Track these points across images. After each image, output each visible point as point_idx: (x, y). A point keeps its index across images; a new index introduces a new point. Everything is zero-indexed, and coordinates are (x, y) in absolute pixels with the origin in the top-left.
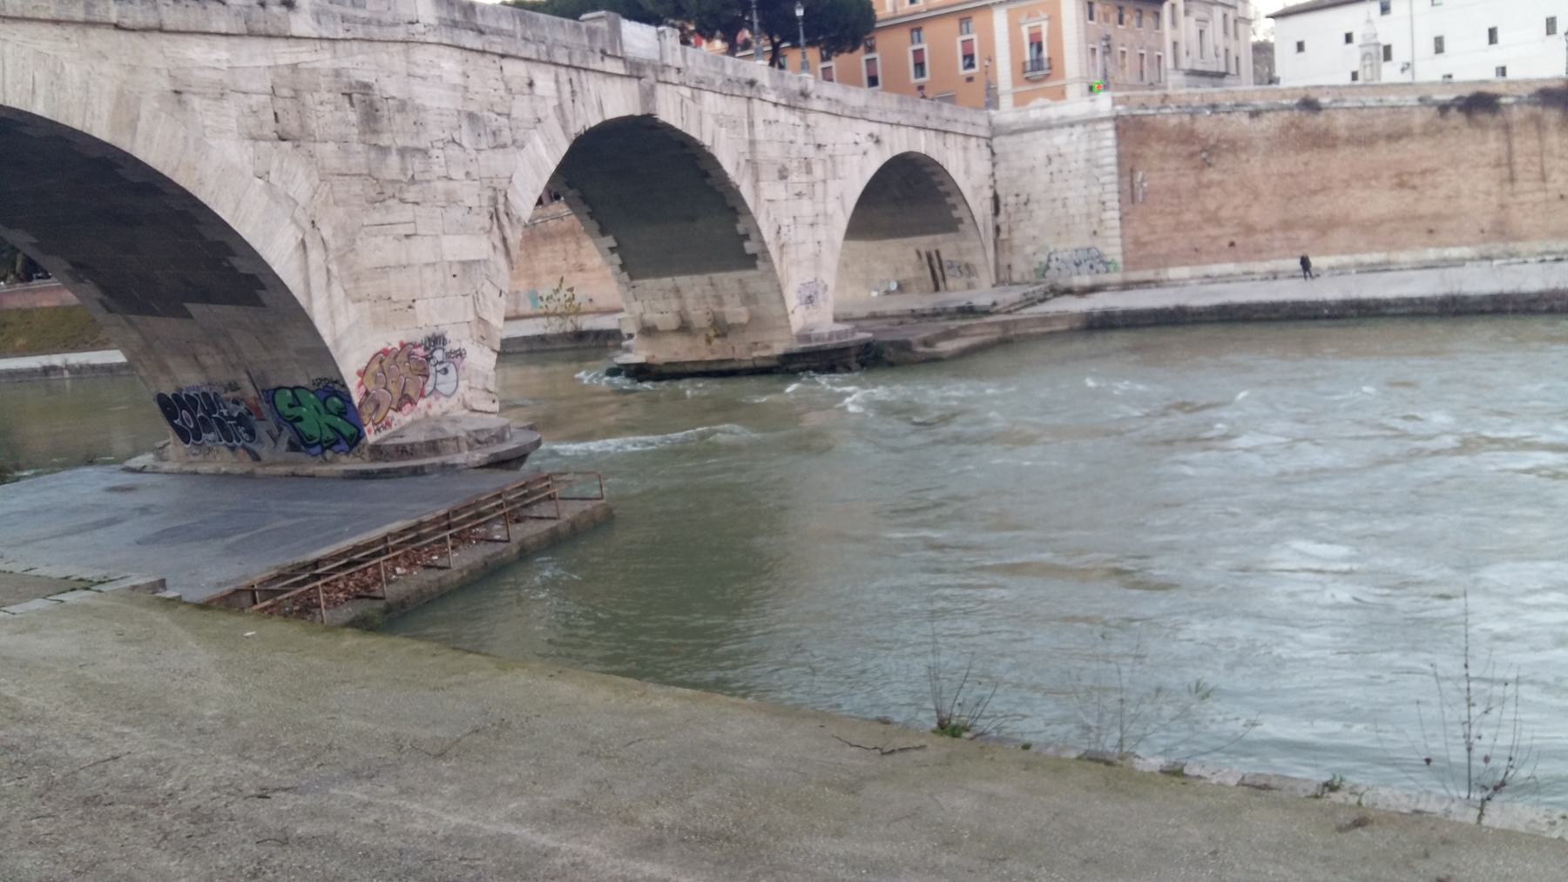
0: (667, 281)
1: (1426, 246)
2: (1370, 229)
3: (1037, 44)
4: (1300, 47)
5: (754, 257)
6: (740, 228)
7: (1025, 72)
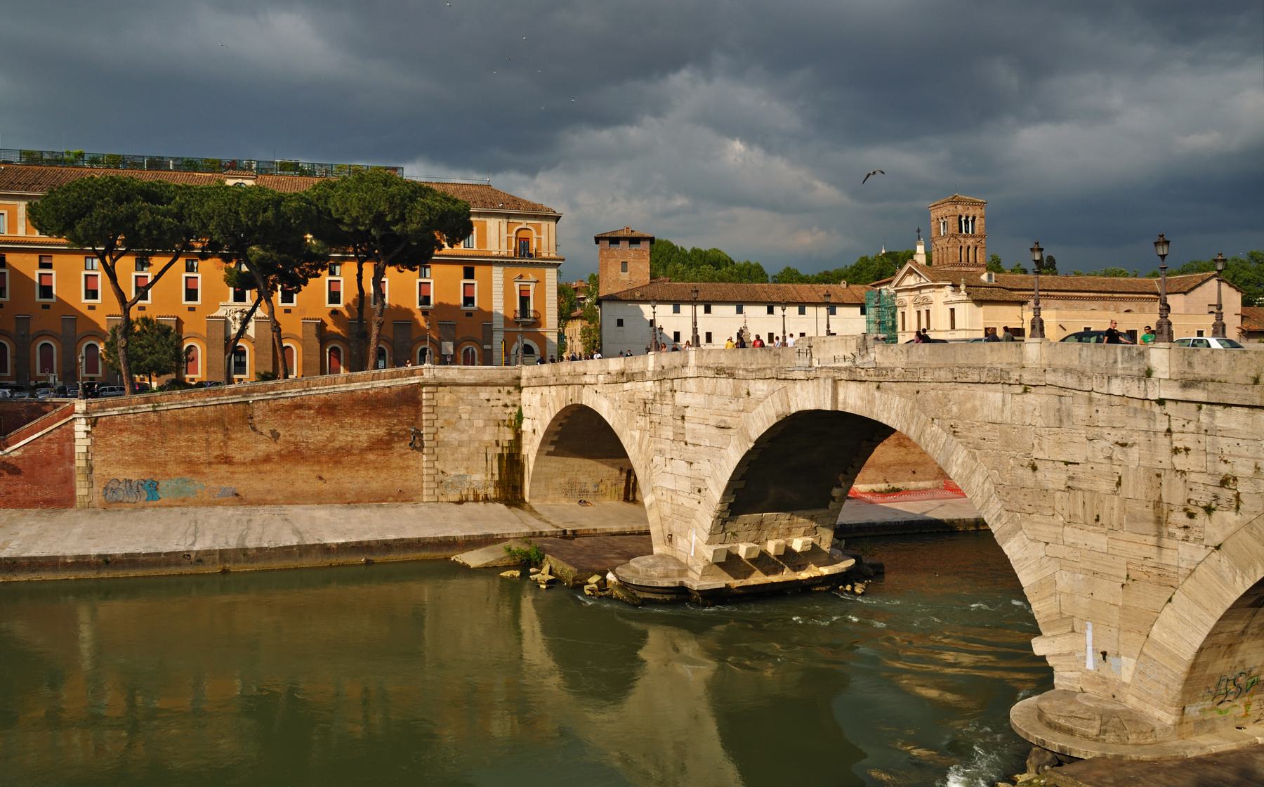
3: (524, 300)
4: (620, 323)
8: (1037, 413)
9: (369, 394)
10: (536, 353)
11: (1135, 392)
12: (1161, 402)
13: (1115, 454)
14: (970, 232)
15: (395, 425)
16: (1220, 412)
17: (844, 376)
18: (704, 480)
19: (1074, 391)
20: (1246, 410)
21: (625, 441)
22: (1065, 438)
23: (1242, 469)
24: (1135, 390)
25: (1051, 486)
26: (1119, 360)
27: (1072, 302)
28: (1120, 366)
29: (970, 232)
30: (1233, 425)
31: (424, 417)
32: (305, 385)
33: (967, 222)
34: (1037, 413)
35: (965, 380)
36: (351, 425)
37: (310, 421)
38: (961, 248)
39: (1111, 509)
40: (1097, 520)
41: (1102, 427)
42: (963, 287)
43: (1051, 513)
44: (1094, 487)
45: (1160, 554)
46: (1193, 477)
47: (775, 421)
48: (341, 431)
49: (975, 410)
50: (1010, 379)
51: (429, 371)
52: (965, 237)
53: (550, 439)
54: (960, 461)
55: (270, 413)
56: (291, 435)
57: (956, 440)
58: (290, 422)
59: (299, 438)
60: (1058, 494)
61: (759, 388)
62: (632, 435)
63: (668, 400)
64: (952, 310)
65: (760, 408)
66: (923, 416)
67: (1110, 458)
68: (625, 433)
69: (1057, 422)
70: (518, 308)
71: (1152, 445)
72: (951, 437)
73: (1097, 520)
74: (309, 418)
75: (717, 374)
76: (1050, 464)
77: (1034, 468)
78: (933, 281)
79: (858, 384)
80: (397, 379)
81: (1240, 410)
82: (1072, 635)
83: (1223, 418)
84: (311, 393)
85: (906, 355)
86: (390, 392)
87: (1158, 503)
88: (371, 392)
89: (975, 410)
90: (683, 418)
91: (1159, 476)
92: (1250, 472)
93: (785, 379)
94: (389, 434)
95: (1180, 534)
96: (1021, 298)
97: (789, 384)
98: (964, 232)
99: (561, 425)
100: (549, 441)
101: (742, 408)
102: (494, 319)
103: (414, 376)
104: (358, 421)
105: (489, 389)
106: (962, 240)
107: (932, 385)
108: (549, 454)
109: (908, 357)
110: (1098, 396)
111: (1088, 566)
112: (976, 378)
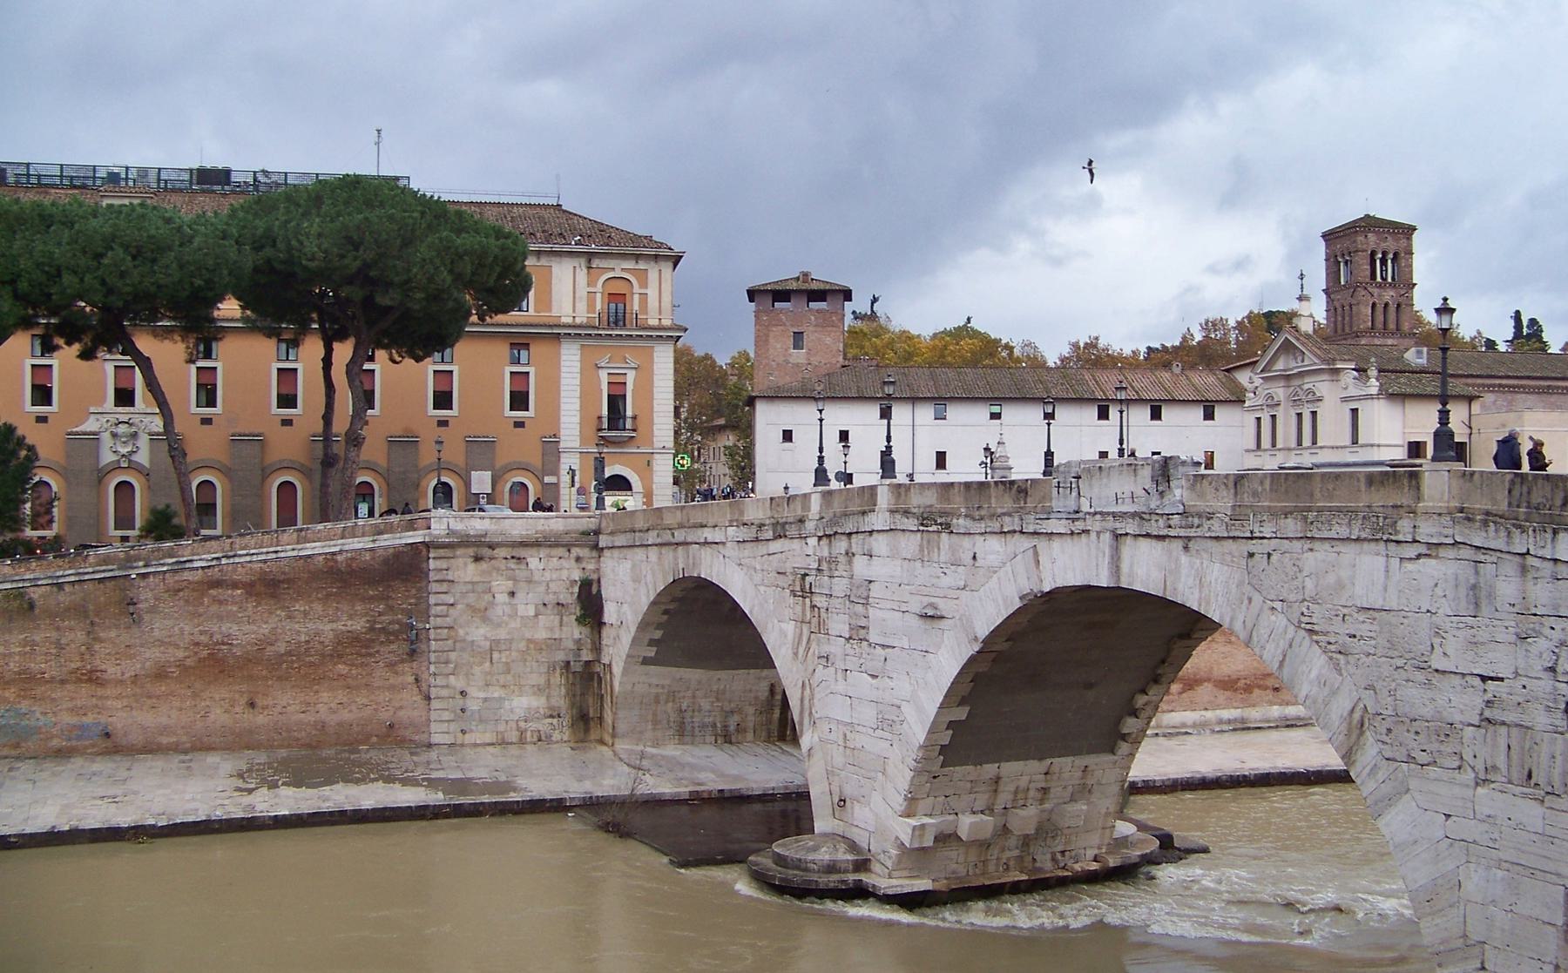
0: (990, 769)
1: (1271, 703)
2: (1229, 685)
4: (787, 436)
5: (1124, 737)
6: (1141, 700)
7: (600, 430)
8: (1439, 591)
9: (336, 561)
10: (634, 490)
13: (1560, 662)
14: (1390, 280)
15: (380, 614)
17: (1131, 527)
19: (1499, 554)
21: (771, 640)
22: (1483, 635)
25: (1457, 718)
27: (1553, 398)
29: (1390, 280)
31: (432, 600)
32: (227, 547)
33: (1384, 262)
34: (1439, 591)
35: (1326, 534)
36: (305, 614)
37: (235, 609)
38: (1374, 305)
41: (1542, 616)
42: (1373, 372)
43: (1456, 764)
47: (1017, 604)
48: (288, 625)
49: (1340, 586)
50: (1397, 532)
51: (443, 522)
52: (1380, 286)
53: (648, 637)
54: (1313, 674)
55: (166, 595)
56: (201, 633)
58: (201, 610)
59: (218, 637)
62: (781, 630)
63: (841, 569)
64: (1355, 411)
66: (1257, 598)
67: (1552, 669)
68: (770, 626)
69: (1472, 607)
70: (605, 412)
74: (234, 603)
75: (922, 525)
76: (1457, 680)
78: (1324, 361)
79: (1154, 542)
80: (386, 536)
84: (237, 560)
85: (1232, 491)
86: (373, 558)
88: (339, 558)
94: (372, 629)
96: (1471, 391)
97: (1042, 544)
98: (1379, 279)
99: (666, 612)
100: (646, 642)
101: (962, 584)
102: (562, 432)
103: (415, 530)
104: (318, 607)
105: (543, 552)
106: (1376, 291)
108: (646, 661)
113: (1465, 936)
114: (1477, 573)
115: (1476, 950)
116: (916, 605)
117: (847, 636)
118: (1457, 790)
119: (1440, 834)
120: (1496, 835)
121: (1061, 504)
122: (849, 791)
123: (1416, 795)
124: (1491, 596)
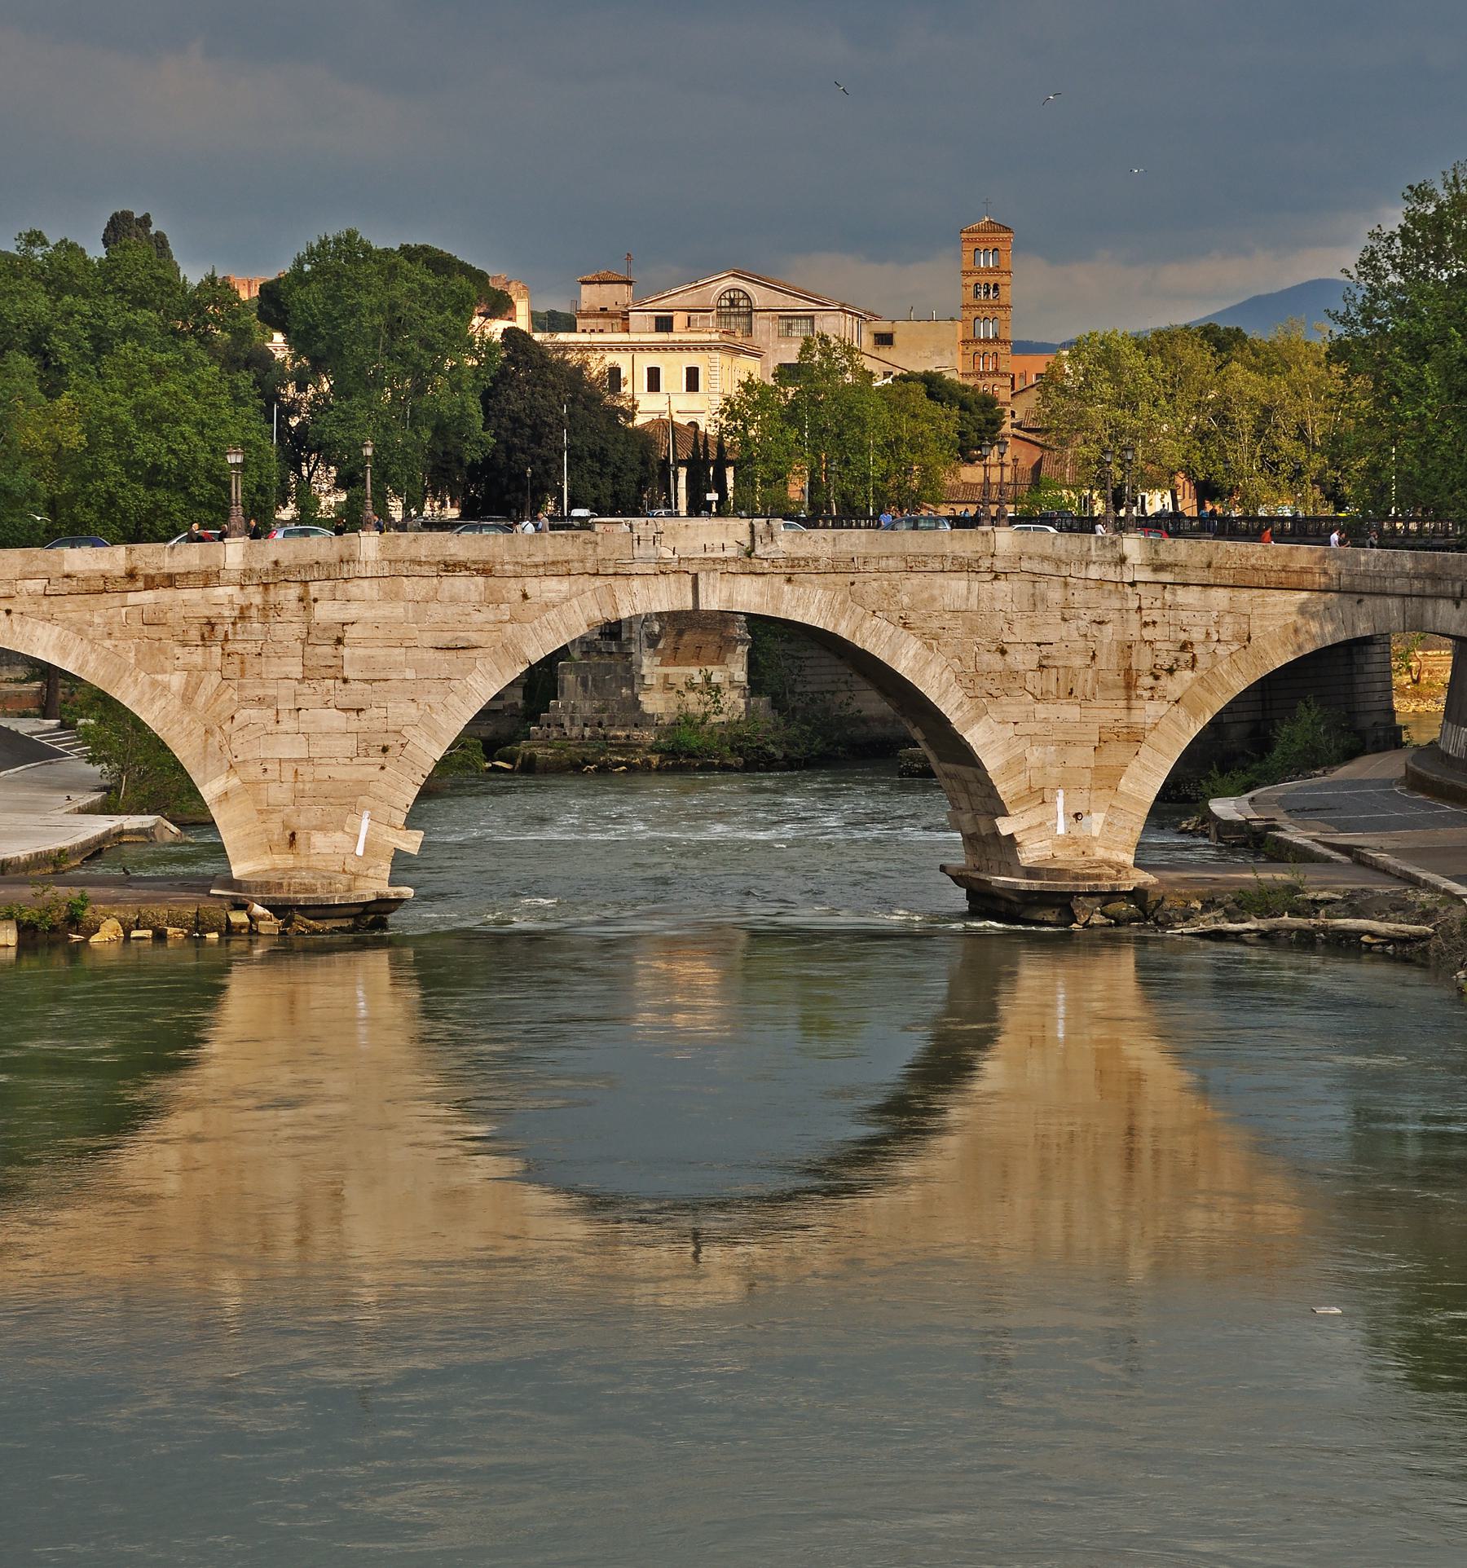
11: (1112, 574)
12: (1133, 584)
16: (1180, 591)
18: (399, 732)
20: (1200, 588)
22: (1038, 621)
23: (1197, 635)
24: (1112, 574)
25: (1022, 667)
26: (1093, 548)
28: (1093, 553)
30: (1191, 601)
35: (923, 569)
39: (1085, 681)
40: (1071, 693)
44: (1069, 663)
45: (1129, 714)
46: (1158, 645)
49: (933, 599)
50: (979, 567)
54: (911, 653)
57: (906, 632)
60: (1030, 674)
61: (554, 588)
65: (552, 615)
66: (859, 609)
71: (1124, 621)
72: (901, 629)
73: (1071, 693)
76: (1021, 647)
77: (1003, 652)
81: (1195, 588)
82: (1042, 806)
83: (1185, 596)
87: (1128, 671)
89: (933, 599)
90: (339, 641)
91: (1130, 647)
92: (1203, 637)
93: (615, 574)
95: (1146, 694)
107: (874, 576)
109: (835, 545)
110: (1074, 580)
111: (1061, 737)
112: (938, 566)
113: (1030, 787)
114: (1034, 587)
115: (1039, 794)
116: (428, 639)
117: (300, 676)
118: (1023, 708)
119: (1012, 734)
120: (1050, 727)
121: (768, 549)
122: (300, 821)
123: (993, 715)
124: (1044, 600)
